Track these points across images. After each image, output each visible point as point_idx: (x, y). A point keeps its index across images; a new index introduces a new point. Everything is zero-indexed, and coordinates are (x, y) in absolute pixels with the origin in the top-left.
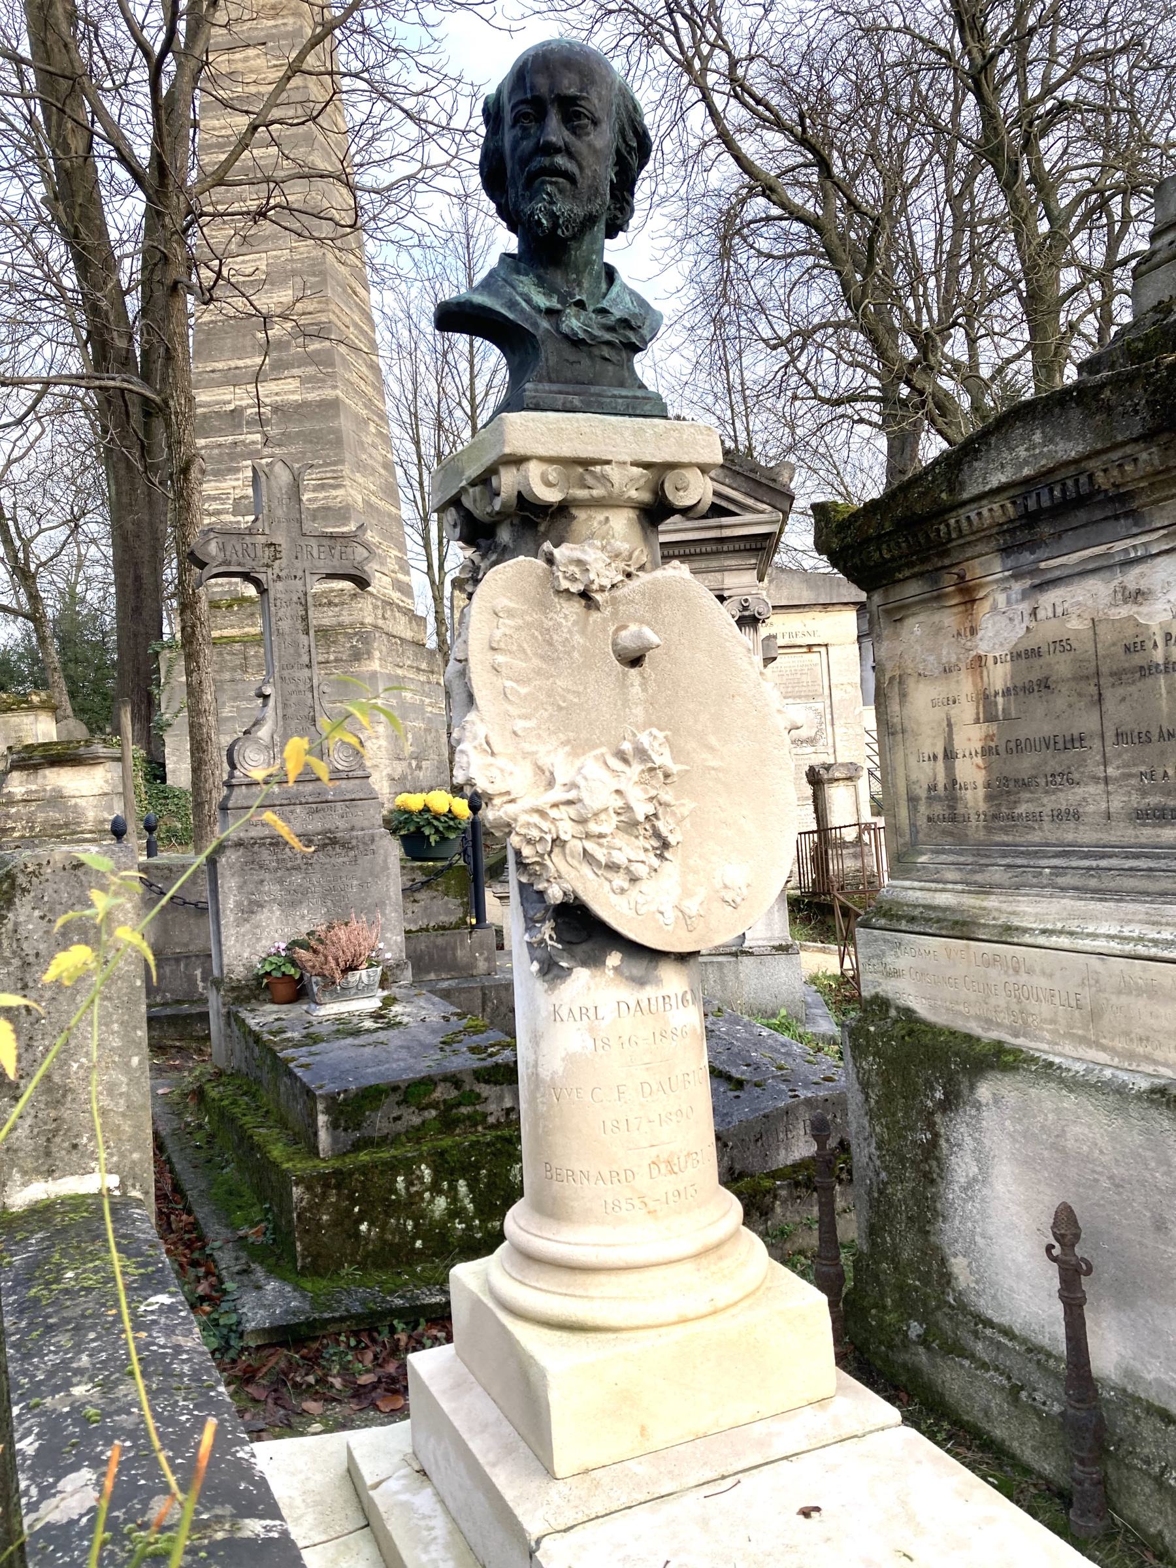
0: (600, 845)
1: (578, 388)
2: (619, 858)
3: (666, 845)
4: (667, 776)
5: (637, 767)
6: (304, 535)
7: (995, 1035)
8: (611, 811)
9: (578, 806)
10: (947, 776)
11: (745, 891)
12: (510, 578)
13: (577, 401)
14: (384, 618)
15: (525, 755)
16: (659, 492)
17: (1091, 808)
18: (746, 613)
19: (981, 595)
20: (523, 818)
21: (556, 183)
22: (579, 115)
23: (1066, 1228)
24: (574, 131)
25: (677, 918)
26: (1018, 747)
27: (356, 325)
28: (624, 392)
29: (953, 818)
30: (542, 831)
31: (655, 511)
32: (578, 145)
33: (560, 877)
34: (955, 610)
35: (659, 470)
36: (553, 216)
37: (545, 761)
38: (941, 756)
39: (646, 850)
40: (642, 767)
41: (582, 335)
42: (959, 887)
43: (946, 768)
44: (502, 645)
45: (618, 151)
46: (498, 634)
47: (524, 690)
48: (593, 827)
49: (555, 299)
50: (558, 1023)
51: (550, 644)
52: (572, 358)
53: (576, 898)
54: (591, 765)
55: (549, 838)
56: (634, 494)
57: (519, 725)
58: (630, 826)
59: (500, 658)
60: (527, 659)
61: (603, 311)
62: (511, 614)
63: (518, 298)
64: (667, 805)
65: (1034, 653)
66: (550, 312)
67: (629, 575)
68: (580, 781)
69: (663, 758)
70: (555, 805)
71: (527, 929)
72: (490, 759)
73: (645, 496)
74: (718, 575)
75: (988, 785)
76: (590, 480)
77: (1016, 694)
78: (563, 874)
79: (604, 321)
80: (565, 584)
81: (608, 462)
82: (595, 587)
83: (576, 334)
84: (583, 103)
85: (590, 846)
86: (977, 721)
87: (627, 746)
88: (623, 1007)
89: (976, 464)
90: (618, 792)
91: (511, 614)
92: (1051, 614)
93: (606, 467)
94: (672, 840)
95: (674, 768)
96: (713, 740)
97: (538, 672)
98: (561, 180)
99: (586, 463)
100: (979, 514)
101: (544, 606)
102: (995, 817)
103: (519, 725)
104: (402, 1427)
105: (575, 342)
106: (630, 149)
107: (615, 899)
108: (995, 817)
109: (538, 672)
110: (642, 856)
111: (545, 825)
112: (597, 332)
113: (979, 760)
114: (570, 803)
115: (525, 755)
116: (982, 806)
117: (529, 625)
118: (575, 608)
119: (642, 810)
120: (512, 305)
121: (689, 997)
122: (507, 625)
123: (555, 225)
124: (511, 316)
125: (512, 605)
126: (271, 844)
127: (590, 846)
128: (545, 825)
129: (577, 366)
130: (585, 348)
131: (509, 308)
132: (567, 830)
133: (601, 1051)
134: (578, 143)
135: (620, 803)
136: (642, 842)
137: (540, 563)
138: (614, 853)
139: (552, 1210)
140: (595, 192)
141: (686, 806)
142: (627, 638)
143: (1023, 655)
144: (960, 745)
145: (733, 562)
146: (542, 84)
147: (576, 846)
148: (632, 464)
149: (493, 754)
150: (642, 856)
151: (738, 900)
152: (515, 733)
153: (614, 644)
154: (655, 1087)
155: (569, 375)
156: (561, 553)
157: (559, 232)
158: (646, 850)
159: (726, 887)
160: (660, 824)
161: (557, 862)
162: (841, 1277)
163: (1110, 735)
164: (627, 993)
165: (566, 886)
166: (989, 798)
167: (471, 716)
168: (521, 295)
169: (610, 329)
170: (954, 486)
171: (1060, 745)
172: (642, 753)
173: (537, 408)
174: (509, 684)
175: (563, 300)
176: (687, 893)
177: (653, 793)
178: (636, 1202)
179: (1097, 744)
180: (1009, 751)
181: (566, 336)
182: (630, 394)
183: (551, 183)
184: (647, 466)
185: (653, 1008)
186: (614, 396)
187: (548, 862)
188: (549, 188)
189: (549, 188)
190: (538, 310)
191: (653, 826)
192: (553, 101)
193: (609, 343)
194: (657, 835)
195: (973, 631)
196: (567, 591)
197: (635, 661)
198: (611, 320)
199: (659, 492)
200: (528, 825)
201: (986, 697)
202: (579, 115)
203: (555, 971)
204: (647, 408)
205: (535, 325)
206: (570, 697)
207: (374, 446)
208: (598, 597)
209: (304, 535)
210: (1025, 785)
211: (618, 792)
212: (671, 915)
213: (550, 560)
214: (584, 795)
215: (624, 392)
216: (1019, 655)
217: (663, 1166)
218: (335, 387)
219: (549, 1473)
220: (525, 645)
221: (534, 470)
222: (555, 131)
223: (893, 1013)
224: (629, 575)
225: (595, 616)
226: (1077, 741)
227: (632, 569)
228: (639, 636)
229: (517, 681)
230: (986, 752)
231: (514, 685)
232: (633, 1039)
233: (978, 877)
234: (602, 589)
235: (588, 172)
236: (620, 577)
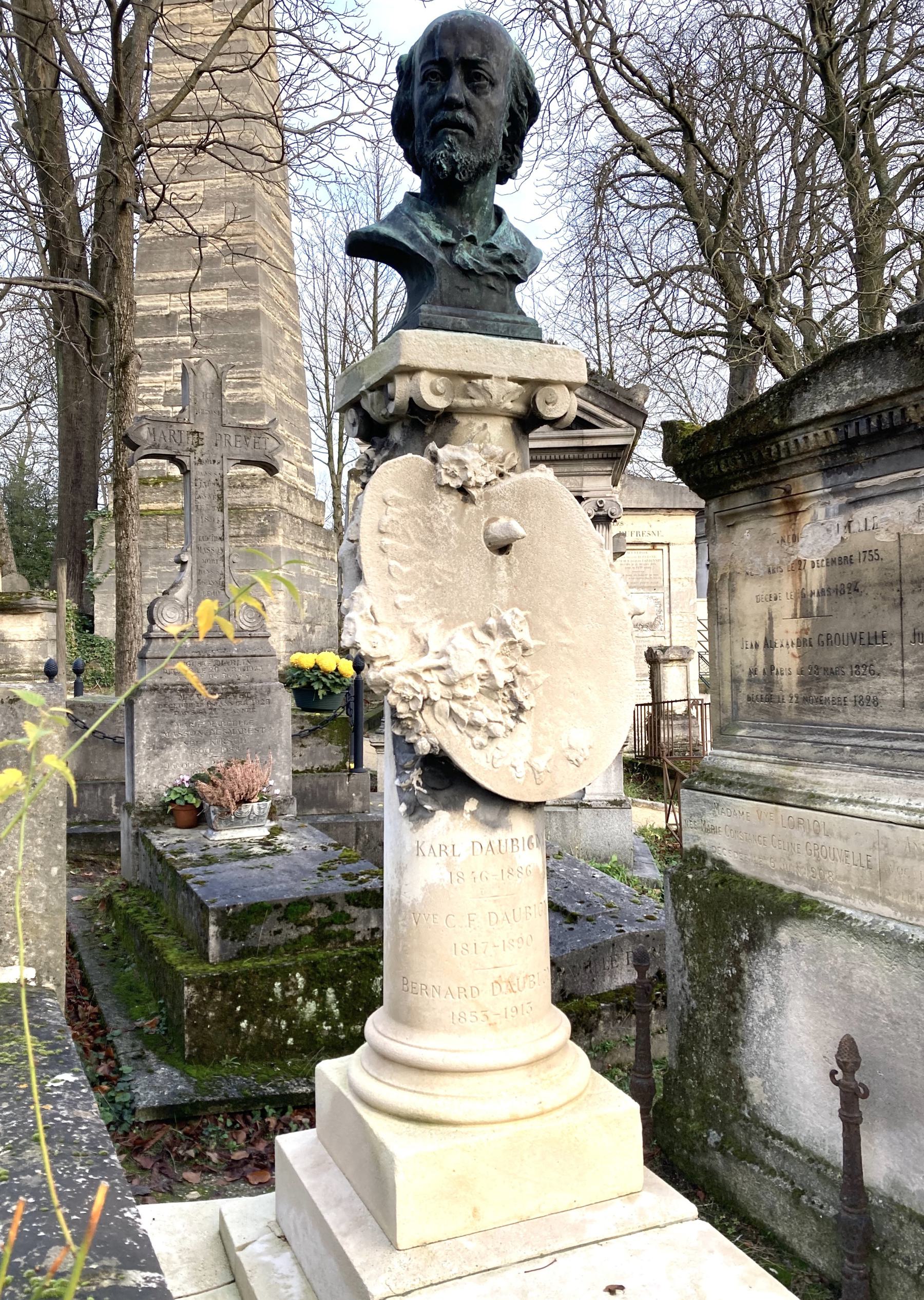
0: (465, 706)
1: (466, 311)
2: (480, 718)
3: (521, 709)
4: (525, 649)
5: (500, 641)
6: (224, 426)
7: (795, 887)
8: (475, 677)
9: (447, 671)
10: (766, 662)
11: (587, 753)
12: (399, 472)
13: (464, 322)
14: (289, 501)
15: (404, 625)
16: (531, 404)
17: (888, 697)
18: (601, 513)
19: (804, 508)
20: (400, 679)
21: (456, 134)
22: (479, 77)
23: (848, 1057)
24: (474, 90)
25: (527, 772)
26: (828, 641)
27: (278, 247)
28: (506, 317)
29: (770, 699)
30: (415, 691)
31: (527, 421)
32: (477, 103)
33: (429, 732)
34: (781, 520)
35: (532, 386)
36: (452, 163)
37: (421, 632)
38: (761, 645)
39: (504, 712)
40: (504, 641)
41: (471, 266)
42: (772, 758)
43: (766, 655)
44: (389, 529)
46: (386, 520)
47: (406, 569)
48: (459, 690)
49: (450, 234)
50: (421, 857)
51: (431, 531)
53: (441, 750)
54: (460, 636)
55: (420, 697)
56: (509, 405)
57: (401, 599)
58: (491, 691)
59: (387, 541)
60: (410, 542)
61: (491, 247)
62: (398, 503)
63: (419, 231)
64: (524, 675)
65: (847, 560)
66: (445, 245)
67: (501, 475)
68: (450, 650)
69: (522, 634)
70: (428, 670)
71: (398, 775)
73: (519, 408)
74: (578, 479)
75: (801, 672)
76: (472, 391)
77: (829, 595)
78: (431, 729)
79: (491, 255)
80: (446, 480)
82: (472, 483)
83: (467, 265)
84: (483, 66)
85: (456, 706)
87: (492, 622)
88: (477, 846)
89: (805, 395)
91: (398, 503)
92: (863, 528)
93: (487, 381)
94: (526, 704)
95: (532, 643)
96: (566, 621)
97: (419, 554)
98: (461, 131)
99: (470, 377)
100: (806, 438)
101: (426, 498)
102: (805, 699)
103: (401, 599)
104: (268, 1198)
105: (465, 272)
107: (475, 753)
108: (805, 699)
109: (419, 554)
110: (500, 717)
111: (418, 686)
112: (485, 264)
113: (794, 650)
114: (440, 668)
115: (404, 625)
116: (795, 690)
117: (413, 514)
118: (454, 500)
119: (502, 677)
120: (413, 237)
121: (534, 840)
122: (395, 512)
123: (454, 170)
124: (412, 247)
125: (399, 495)
126: (181, 690)
127: (456, 706)
128: (418, 686)
129: (466, 293)
130: (473, 278)
131: (411, 239)
132: (437, 691)
133: (455, 883)
134: (477, 100)
135: (484, 671)
136: (500, 705)
137: (426, 460)
138: (477, 713)
139: (406, 1018)
140: (490, 143)
141: (540, 676)
142: (497, 529)
143: (837, 562)
144: (779, 635)
145: (592, 469)
146: (449, 48)
147: (443, 705)
148: (510, 379)
149: (376, 623)
150: (500, 717)
151: (581, 759)
152: (396, 606)
153: (486, 533)
154: (501, 916)
155: (459, 300)
156: (444, 453)
157: (457, 176)
158: (504, 712)
159: (571, 747)
160: (517, 691)
161: (426, 719)
162: (652, 1089)
163: (908, 634)
164: (481, 835)
165: (434, 740)
166: (801, 683)
167: (360, 589)
168: (421, 228)
169: (497, 262)
170: (785, 412)
171: (865, 641)
172: (505, 629)
173: (430, 327)
174: (393, 563)
175: (457, 235)
176: (537, 751)
177: (512, 663)
178: (480, 1015)
179: (896, 641)
181: (458, 267)
182: (511, 319)
183: (452, 134)
184: (522, 381)
185: (503, 849)
186: (497, 320)
187: (419, 719)
188: (450, 138)
189: (450, 138)
190: (435, 242)
191: (511, 692)
192: (457, 63)
193: (494, 274)
194: (514, 699)
195: (795, 539)
196: (448, 485)
197: (503, 549)
198: (497, 255)
199: (531, 404)
201: (804, 596)
202: (479, 77)
203: (420, 812)
204: (525, 332)
205: (432, 255)
206: (445, 577)
207: (288, 352)
208: (474, 492)
209: (224, 426)
210: (833, 673)
211: (482, 661)
212: (522, 769)
213: (434, 459)
214: (453, 662)
215: (506, 317)
216: (833, 561)
217: (504, 986)
218: (257, 300)
219: (393, 1244)
220: (409, 531)
221: (424, 379)
222: (458, 89)
223: (709, 864)
224: (501, 475)
225: (470, 508)
226: (878, 638)
227: (504, 470)
228: (508, 528)
229: (401, 561)
230: (801, 643)
231: (398, 564)
232: (484, 874)
233: (789, 751)
234: (478, 486)
235: (485, 126)
236: (494, 476)
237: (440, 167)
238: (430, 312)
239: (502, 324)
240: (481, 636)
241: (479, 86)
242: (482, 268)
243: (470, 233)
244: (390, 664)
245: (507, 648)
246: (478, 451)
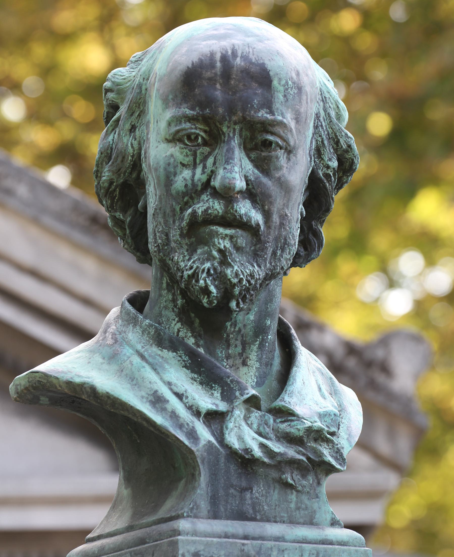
22: (267, 144)
41: (258, 452)
52: (244, 484)
83: (248, 451)
105: (245, 462)
112: (277, 447)
120: (157, 401)
124: (158, 419)
168: (169, 384)
175: (228, 395)
181: (232, 453)
193: (293, 463)
205: (192, 434)
222: (238, 171)
235: (276, 218)
238: (195, 533)
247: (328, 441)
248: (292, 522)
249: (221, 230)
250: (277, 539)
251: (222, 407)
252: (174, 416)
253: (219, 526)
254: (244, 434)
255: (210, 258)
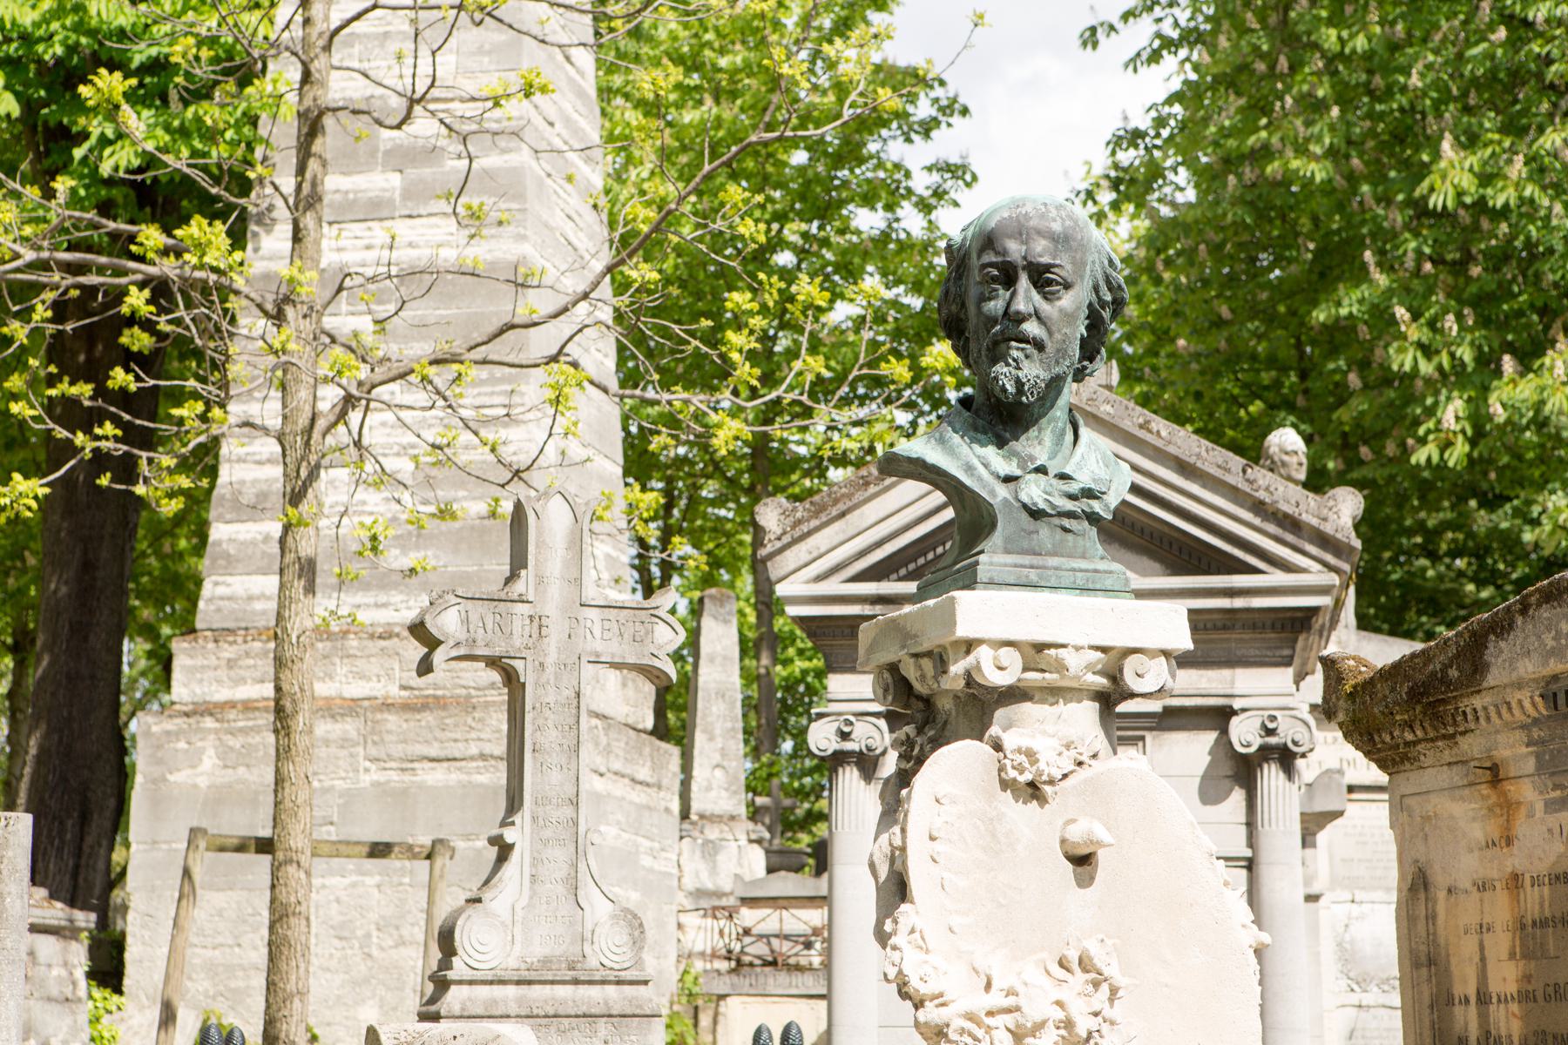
1: (1036, 560)
10: (1480, 1026)
18: (1273, 740)
22: (1050, 282)
24: (1047, 297)
27: (568, 121)
28: (1083, 564)
31: (1108, 700)
36: (1019, 384)
38: (1473, 1000)
41: (1042, 505)
45: (1090, 305)
49: (1014, 463)
52: (1032, 528)
61: (1063, 477)
64: (1112, 1023)
66: (1008, 479)
67: (1080, 764)
68: (1020, 988)
70: (990, 1014)
72: (923, 956)
73: (1102, 682)
80: (1012, 774)
81: (1063, 646)
82: (1045, 778)
83: (1035, 504)
86: (1512, 956)
87: (1073, 955)
89: (1502, 644)
90: (1059, 1004)
93: (1061, 651)
99: (1040, 647)
106: (1103, 304)
113: (1514, 1007)
114: (1008, 1011)
120: (969, 469)
135: (1060, 1015)
140: (1062, 352)
142: (1076, 834)
144: (1494, 987)
145: (1252, 652)
148: (1092, 648)
149: (927, 951)
153: (1063, 841)
167: (904, 907)
172: (1085, 964)
180: (1547, 998)
181: (1025, 506)
182: (1091, 566)
184: (1104, 650)
186: (1074, 570)
188: (1015, 353)
189: (1015, 353)
192: (1024, 268)
193: (1070, 515)
195: (1509, 842)
198: (1074, 488)
199: (1115, 677)
200: (962, 1031)
202: (1050, 282)
205: (993, 493)
208: (1048, 789)
211: (1059, 1004)
213: (998, 747)
214: (1021, 1001)
215: (1083, 564)
216: (1557, 878)
218: (522, 238)
221: (984, 654)
224: (1080, 764)
227: (1084, 758)
230: (1525, 997)
235: (1058, 336)
236: (1073, 767)
237: (1004, 389)
238: (991, 564)
239: (1079, 574)
240: (1061, 974)
241: (1053, 293)
242: (1053, 506)
243: (1039, 463)
244: (943, 1005)
245: (1091, 988)
246: (1052, 732)
247: (1098, 498)
248: (1070, 556)
249: (1014, 344)
250: (1056, 569)
251: (1018, 472)
252: (980, 479)
253: (1011, 559)
254: (1034, 491)
255: (1008, 365)
